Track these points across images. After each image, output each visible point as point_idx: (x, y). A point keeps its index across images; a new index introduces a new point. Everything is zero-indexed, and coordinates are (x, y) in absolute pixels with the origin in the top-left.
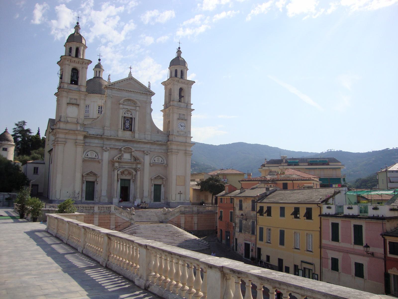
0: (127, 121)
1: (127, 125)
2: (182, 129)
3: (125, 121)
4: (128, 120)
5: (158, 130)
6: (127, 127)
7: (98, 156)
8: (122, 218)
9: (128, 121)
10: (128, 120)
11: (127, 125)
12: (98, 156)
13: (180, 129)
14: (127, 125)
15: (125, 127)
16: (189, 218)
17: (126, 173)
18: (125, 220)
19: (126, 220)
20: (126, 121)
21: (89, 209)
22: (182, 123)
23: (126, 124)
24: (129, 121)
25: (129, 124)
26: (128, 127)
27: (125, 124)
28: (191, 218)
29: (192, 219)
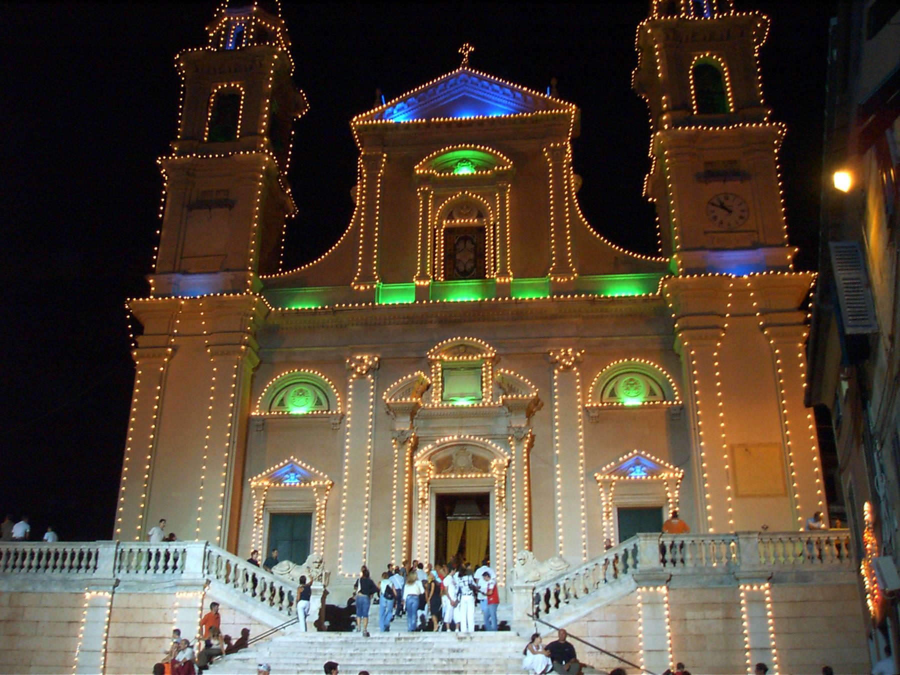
0: (462, 244)
1: (465, 261)
2: (729, 224)
3: (455, 245)
4: (465, 239)
5: (616, 258)
6: (462, 269)
7: (328, 402)
8: (243, 613)
9: (469, 245)
10: (469, 238)
11: (465, 258)
12: (328, 402)
13: (721, 223)
14: (465, 261)
15: (455, 267)
16: (709, 614)
17: (462, 462)
18: (260, 623)
19: (267, 625)
20: (457, 243)
21: (75, 562)
22: (727, 199)
23: (458, 256)
24: (473, 243)
25: (472, 256)
26: (470, 265)
27: (455, 256)
28: (719, 613)
29: (727, 618)
